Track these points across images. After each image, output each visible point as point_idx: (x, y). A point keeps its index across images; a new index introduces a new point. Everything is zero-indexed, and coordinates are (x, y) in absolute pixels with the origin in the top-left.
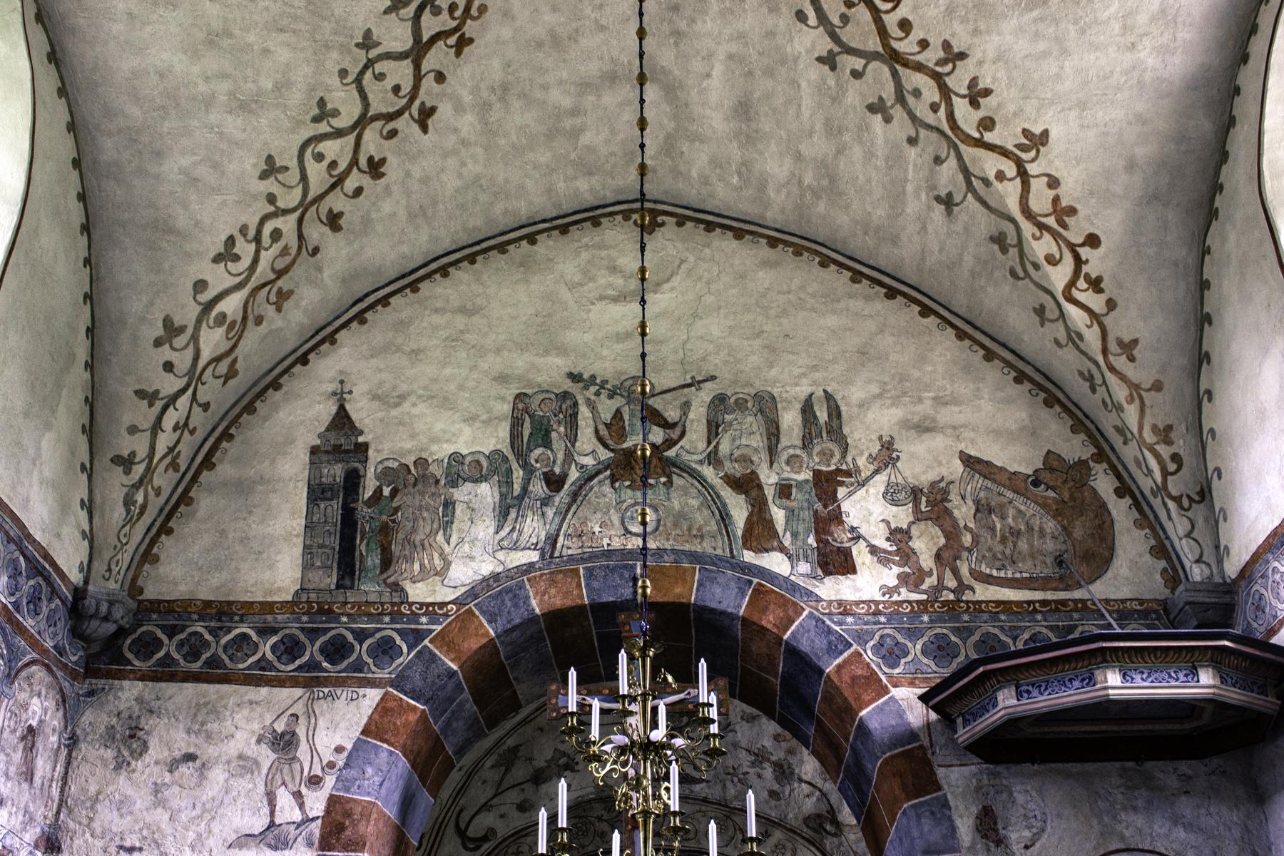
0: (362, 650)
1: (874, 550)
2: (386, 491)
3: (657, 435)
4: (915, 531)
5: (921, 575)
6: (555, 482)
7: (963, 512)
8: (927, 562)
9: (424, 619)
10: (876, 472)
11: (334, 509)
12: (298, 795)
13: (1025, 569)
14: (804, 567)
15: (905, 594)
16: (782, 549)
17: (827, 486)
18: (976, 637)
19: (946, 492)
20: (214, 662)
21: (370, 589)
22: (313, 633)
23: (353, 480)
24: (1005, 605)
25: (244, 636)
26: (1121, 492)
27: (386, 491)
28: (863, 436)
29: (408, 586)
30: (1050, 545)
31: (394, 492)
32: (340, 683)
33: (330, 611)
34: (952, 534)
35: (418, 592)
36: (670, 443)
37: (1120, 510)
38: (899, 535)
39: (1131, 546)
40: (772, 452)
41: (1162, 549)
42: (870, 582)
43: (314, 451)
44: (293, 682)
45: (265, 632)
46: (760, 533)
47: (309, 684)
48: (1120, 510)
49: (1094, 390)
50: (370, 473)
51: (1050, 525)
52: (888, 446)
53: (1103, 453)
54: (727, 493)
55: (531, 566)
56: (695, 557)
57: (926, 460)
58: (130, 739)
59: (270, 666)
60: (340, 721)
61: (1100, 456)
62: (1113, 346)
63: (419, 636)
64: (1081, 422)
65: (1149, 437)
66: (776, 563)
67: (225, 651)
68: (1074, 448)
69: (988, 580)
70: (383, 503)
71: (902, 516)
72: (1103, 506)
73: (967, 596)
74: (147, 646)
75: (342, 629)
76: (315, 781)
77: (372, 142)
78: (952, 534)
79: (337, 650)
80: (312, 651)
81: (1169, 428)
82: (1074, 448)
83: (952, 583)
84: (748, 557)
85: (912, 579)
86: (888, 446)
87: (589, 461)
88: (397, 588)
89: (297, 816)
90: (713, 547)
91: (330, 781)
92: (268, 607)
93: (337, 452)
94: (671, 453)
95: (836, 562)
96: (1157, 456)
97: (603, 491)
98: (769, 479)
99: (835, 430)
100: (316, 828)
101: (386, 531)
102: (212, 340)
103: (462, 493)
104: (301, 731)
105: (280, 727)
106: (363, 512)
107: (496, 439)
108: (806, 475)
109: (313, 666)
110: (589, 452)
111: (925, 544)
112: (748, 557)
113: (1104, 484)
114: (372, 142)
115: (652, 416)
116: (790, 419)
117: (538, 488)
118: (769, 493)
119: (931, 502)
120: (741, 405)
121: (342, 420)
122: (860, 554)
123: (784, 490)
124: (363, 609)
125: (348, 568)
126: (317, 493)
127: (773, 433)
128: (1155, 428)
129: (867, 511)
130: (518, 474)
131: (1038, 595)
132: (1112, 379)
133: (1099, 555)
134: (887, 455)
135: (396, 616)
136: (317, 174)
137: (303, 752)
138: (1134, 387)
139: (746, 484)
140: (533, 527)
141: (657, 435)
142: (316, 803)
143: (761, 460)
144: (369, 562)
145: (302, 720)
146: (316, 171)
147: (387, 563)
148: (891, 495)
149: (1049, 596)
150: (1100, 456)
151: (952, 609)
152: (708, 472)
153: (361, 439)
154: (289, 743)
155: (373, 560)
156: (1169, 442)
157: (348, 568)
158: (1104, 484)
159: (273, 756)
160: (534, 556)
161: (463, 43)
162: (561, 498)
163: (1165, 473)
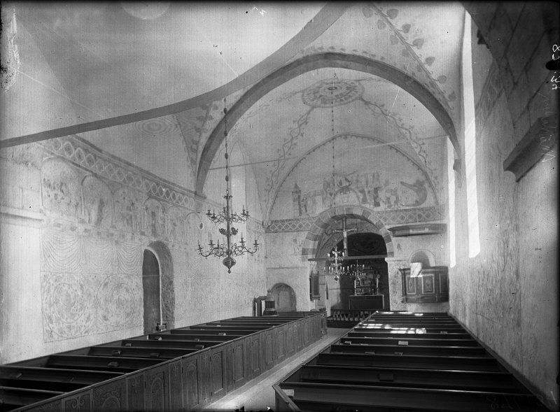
3: (347, 184)
5: (392, 205)
7: (399, 193)
17: (376, 190)
23: (299, 196)
28: (383, 179)
30: (415, 199)
34: (397, 198)
36: (350, 185)
40: (367, 184)
41: (435, 197)
42: (383, 207)
46: (365, 201)
54: (359, 194)
58: (274, 242)
60: (303, 236)
64: (425, 173)
65: (433, 179)
66: (367, 206)
71: (388, 195)
72: (425, 190)
74: (273, 228)
76: (300, 246)
77: (295, 141)
78: (397, 198)
82: (422, 178)
84: (363, 205)
85: (390, 207)
88: (308, 215)
90: (357, 203)
92: (290, 220)
95: (377, 204)
98: (366, 190)
99: (378, 179)
101: (305, 206)
102: (274, 179)
107: (321, 187)
108: (373, 189)
111: (393, 199)
112: (363, 205)
113: (426, 185)
114: (295, 141)
115: (346, 179)
116: (370, 178)
117: (329, 196)
118: (366, 193)
119: (394, 192)
121: (296, 186)
122: (381, 202)
123: (369, 192)
126: (294, 201)
127: (367, 182)
129: (382, 195)
133: (424, 199)
134: (387, 183)
135: (308, 219)
136: (286, 150)
139: (362, 192)
140: (328, 203)
142: (301, 249)
146: (286, 150)
151: (396, 211)
157: (300, 213)
158: (426, 185)
161: (306, 123)
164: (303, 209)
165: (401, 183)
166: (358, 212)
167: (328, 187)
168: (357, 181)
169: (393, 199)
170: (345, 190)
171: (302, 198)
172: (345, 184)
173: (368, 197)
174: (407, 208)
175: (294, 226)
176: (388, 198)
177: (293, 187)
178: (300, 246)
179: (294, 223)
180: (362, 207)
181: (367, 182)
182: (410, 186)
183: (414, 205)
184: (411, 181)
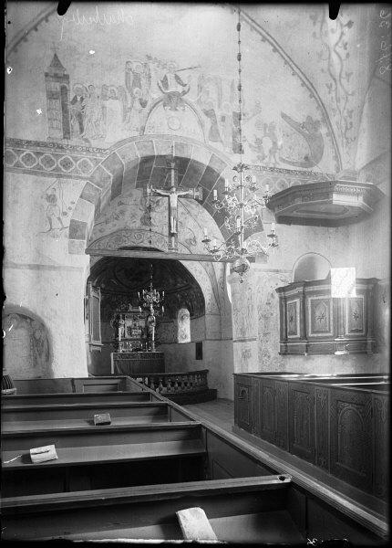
0: (76, 165)
1: (250, 146)
2: (79, 99)
3: (180, 89)
4: (264, 139)
6: (143, 104)
7: (278, 133)
8: (267, 153)
9: (98, 155)
10: (254, 115)
11: (58, 104)
12: (59, 219)
13: (295, 158)
14: (228, 150)
15: (259, 164)
16: (222, 141)
17: (238, 117)
18: (279, 181)
19: (274, 128)
20: (18, 165)
21: (74, 141)
22: (57, 156)
23: (64, 90)
24: (288, 171)
25: (29, 155)
26: (328, 135)
27: (79, 99)
29: (92, 141)
31: (82, 99)
32: (70, 177)
33: (62, 148)
35: (94, 143)
36: (184, 93)
37: (327, 140)
38: (259, 141)
39: (328, 152)
43: (47, 75)
44: (51, 175)
45: (38, 154)
47: (60, 176)
48: (327, 140)
49: (330, 93)
50: (71, 87)
51: (306, 144)
52: (258, 105)
53: (326, 118)
54: (204, 117)
55: (133, 139)
56: (193, 141)
57: (271, 115)
59: (41, 168)
61: (324, 121)
62: (344, 75)
63: (97, 161)
64: (321, 106)
67: (23, 160)
68: (317, 116)
69: (283, 161)
70: (78, 103)
73: (277, 166)
75: (68, 155)
76: (65, 214)
79: (67, 164)
80: (58, 163)
81: (352, 111)
82: (317, 116)
83: (273, 160)
86: (258, 105)
87: (155, 96)
88: (87, 140)
89: (60, 226)
91: (70, 213)
92: (37, 144)
93: (56, 77)
94: (185, 97)
96: (345, 120)
97: (160, 107)
98: (218, 113)
100: (67, 231)
101: (80, 116)
103: (108, 103)
104: (57, 195)
105: (50, 193)
106: (70, 107)
109: (57, 169)
110: (156, 94)
111: (267, 144)
117: (137, 105)
118: (219, 119)
119: (269, 129)
120: (209, 80)
122: (245, 146)
123: (223, 119)
124: (73, 148)
125: (67, 134)
126: (51, 96)
127: (220, 95)
128: (348, 112)
129: (249, 130)
130: (129, 98)
131: (298, 169)
132: (339, 87)
137: (59, 202)
138: (347, 93)
139: (209, 113)
140: (136, 120)
141: (180, 89)
142: (67, 223)
143: (216, 104)
144: (75, 128)
145: (58, 191)
147: (82, 130)
148: (258, 125)
149: (301, 169)
150: (324, 121)
151: (272, 169)
152: (198, 108)
153: (65, 73)
154: (53, 199)
155: (77, 127)
156: (351, 117)
157: (67, 134)
158: (323, 130)
159: (48, 204)
160: (137, 134)
162: (146, 110)
163: (347, 129)
164: (74, 124)
165: (284, 116)
166: (201, 156)
167: (134, 85)
168: (200, 88)
169: (267, 144)
170: (172, 100)
171: (71, 96)
172: (174, 87)
173: (220, 126)
174: (292, 168)
175: (49, 162)
176: (259, 141)
177: (48, 62)
178: (65, 214)
179: (48, 153)
180: (209, 148)
181: (220, 95)
182: (300, 128)
183: (302, 165)
184: (299, 118)
